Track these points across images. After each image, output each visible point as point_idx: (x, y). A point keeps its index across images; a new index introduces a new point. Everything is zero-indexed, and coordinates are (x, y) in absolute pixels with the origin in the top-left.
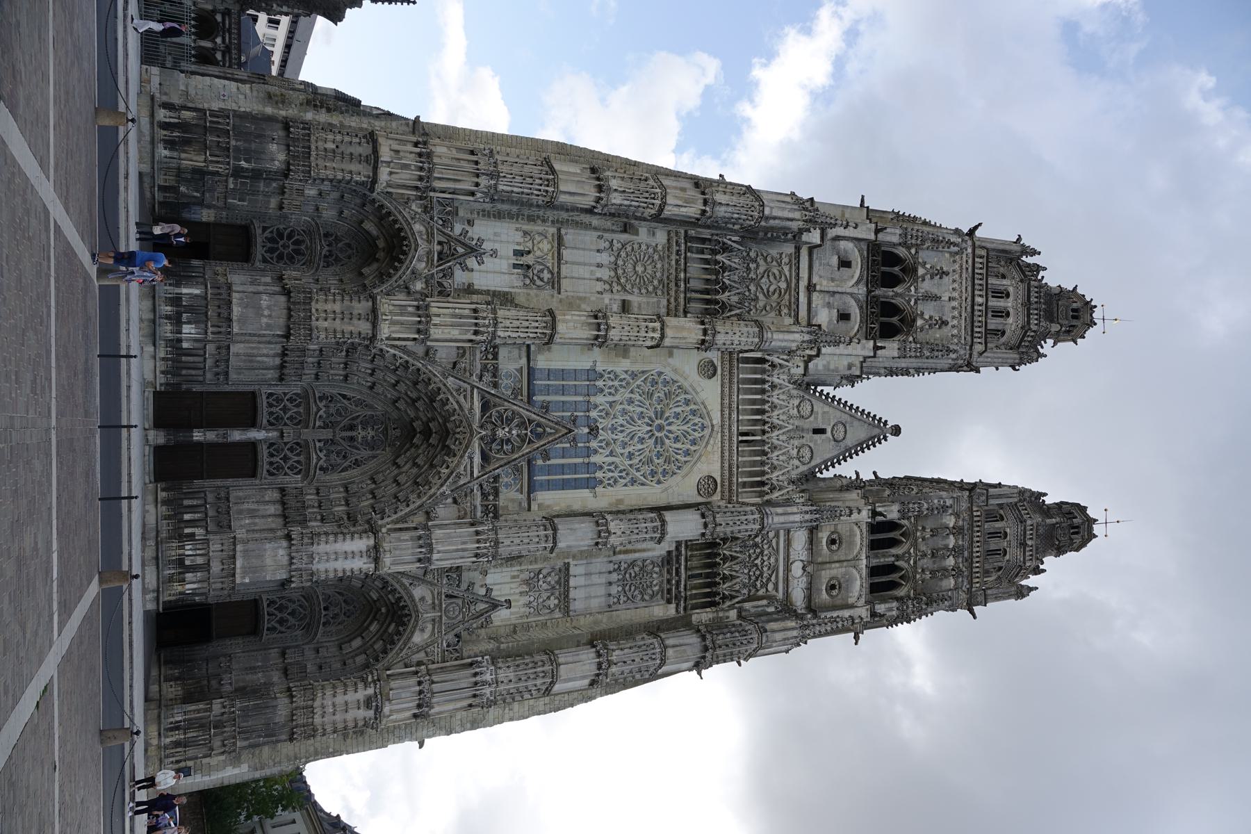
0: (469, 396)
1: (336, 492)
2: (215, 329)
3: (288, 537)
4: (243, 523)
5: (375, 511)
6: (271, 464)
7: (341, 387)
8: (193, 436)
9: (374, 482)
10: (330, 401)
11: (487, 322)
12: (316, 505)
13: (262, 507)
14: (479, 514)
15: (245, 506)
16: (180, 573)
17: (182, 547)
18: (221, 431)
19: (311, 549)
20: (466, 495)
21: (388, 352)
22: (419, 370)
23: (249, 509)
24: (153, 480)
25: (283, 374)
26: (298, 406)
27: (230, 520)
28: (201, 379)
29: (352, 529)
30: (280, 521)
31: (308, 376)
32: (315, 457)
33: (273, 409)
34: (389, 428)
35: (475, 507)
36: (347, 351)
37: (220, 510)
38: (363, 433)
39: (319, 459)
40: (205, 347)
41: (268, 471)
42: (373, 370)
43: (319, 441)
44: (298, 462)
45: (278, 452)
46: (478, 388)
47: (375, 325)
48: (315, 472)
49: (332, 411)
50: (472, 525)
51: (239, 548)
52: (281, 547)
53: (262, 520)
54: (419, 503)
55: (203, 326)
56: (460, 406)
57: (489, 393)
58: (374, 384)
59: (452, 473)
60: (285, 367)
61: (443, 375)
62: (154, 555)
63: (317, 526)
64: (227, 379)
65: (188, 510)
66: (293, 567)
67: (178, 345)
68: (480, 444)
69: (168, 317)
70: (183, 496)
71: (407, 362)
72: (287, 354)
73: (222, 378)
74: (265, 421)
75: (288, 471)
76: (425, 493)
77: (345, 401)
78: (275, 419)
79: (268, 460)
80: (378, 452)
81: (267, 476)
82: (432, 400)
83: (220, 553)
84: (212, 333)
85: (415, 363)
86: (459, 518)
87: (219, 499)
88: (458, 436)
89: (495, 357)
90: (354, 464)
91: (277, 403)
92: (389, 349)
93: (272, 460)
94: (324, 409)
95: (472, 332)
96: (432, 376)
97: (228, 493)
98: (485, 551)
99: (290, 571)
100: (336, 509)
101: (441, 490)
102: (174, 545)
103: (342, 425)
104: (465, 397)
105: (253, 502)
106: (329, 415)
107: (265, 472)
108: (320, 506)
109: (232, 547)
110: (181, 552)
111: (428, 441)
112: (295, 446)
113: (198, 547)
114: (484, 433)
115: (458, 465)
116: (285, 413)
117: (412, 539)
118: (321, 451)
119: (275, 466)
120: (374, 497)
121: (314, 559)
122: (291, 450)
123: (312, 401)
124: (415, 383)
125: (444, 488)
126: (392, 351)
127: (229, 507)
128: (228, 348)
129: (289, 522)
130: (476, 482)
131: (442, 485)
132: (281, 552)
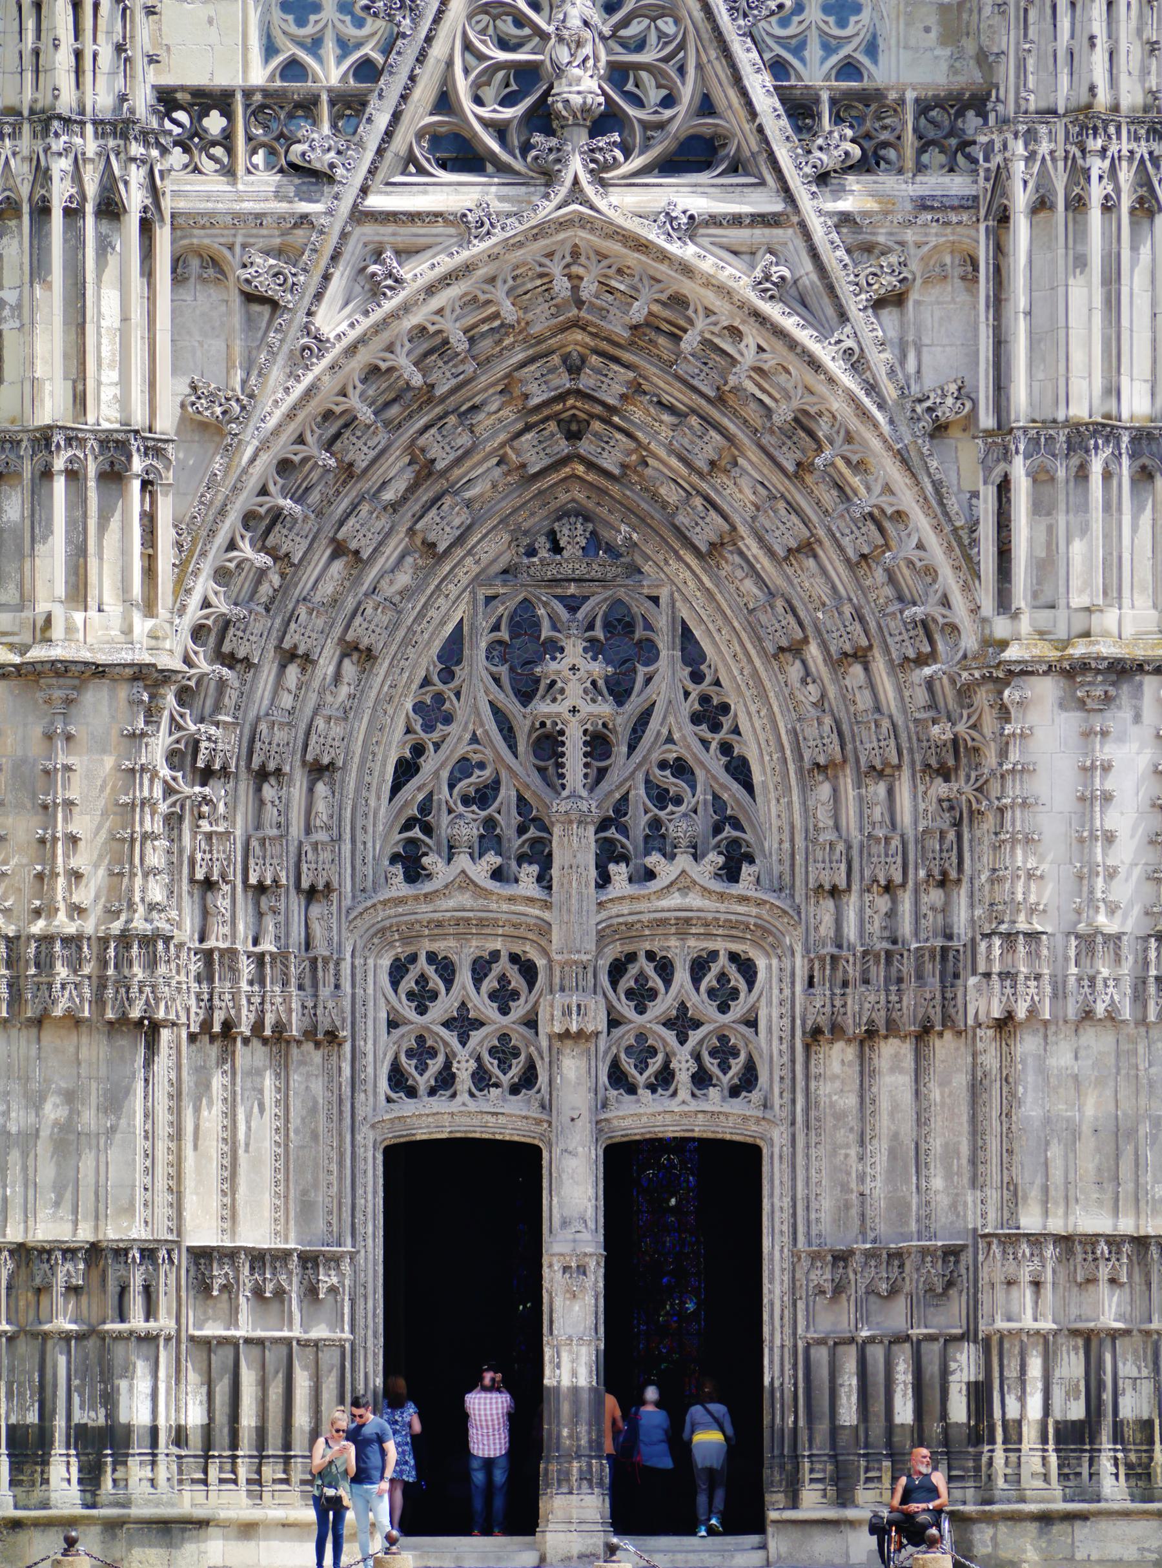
0: (405, 234)
1: (836, 817)
2: (136, 1305)
3: (1005, 1024)
4: (942, 1201)
5: (921, 661)
6: (701, 1079)
7: (363, 786)
8: (575, 1390)
9: (796, 650)
10: (428, 830)
11: (61, 166)
12: (883, 903)
13: (884, 1123)
14: (958, 185)
15: (878, 1188)
16: (1118, 1436)
17: (1013, 1433)
18: (553, 1278)
19: (1059, 937)
20: (868, 249)
21: (206, 604)
22: (284, 466)
23: (891, 1171)
24: (754, 1539)
25: (310, 1034)
26: (447, 970)
27: (924, 1252)
28: (330, 1358)
29: (990, 758)
30: (944, 1047)
31: (317, 930)
32: (675, 900)
33: (464, 1070)
34: (552, 571)
35: (923, 205)
36: (206, 775)
37: (883, 1287)
38: (574, 692)
39: (683, 884)
40: (206, 1344)
41: (734, 1092)
42: (289, 656)
43: (604, 880)
44: (699, 968)
45: (653, 1052)
46: (364, 191)
47: (99, 671)
48: (743, 899)
49: (468, 829)
50: (1004, 218)
51: (1030, 1221)
52: (1041, 1059)
53: (938, 1123)
54: (892, 470)
55: (119, 1349)
56: (447, 279)
57: (389, 134)
58: (350, 649)
59: (756, 314)
60: (280, 1028)
61: (303, 356)
62: (1032, 1528)
63: (972, 906)
64: (335, 1260)
65: (878, 1407)
66: (1126, 1013)
67: (195, 1441)
68: (630, 181)
69: (90, 1478)
70: (823, 1427)
71: (249, 519)
72: (227, 1025)
73: (327, 1279)
74: (516, 1106)
75: (738, 1009)
76: (849, 438)
77: (429, 764)
78: (504, 1066)
79: (684, 1094)
80: (662, 622)
81: (755, 1096)
82: (427, 394)
83: (1048, 1291)
84: (150, 1312)
85: (253, 482)
86: (970, 279)
87: (839, 1289)
88: (588, 289)
89: (221, 100)
90: (715, 727)
91: (433, 1053)
92: (195, 600)
93: (683, 1077)
94: (463, 861)
95: (105, 226)
96: (315, 407)
97: (815, 1257)
98: (1126, 175)
99: (1143, 1021)
100: (905, 815)
101: (837, 368)
102: (999, 1456)
103: (535, 780)
104: (404, 253)
105: (861, 1159)
106: (489, 838)
107: (736, 1106)
108: (888, 888)
109: (1025, 1248)
110: (1030, 1434)
111: (612, 410)
112: (628, 982)
113: (1012, 1372)
114: (576, 165)
115: (724, 291)
116: (479, 1024)
117: (1039, 508)
118: (650, 875)
119: (711, 1064)
120: (861, 656)
121: (1097, 931)
122: (642, 996)
123: (425, 911)
124: (348, 471)
125: (823, 352)
126: (203, 585)
127: (869, 1255)
128: (202, 1256)
129: (947, 1020)
130: (806, 203)
131: (815, 364)
132: (1062, 1057)
